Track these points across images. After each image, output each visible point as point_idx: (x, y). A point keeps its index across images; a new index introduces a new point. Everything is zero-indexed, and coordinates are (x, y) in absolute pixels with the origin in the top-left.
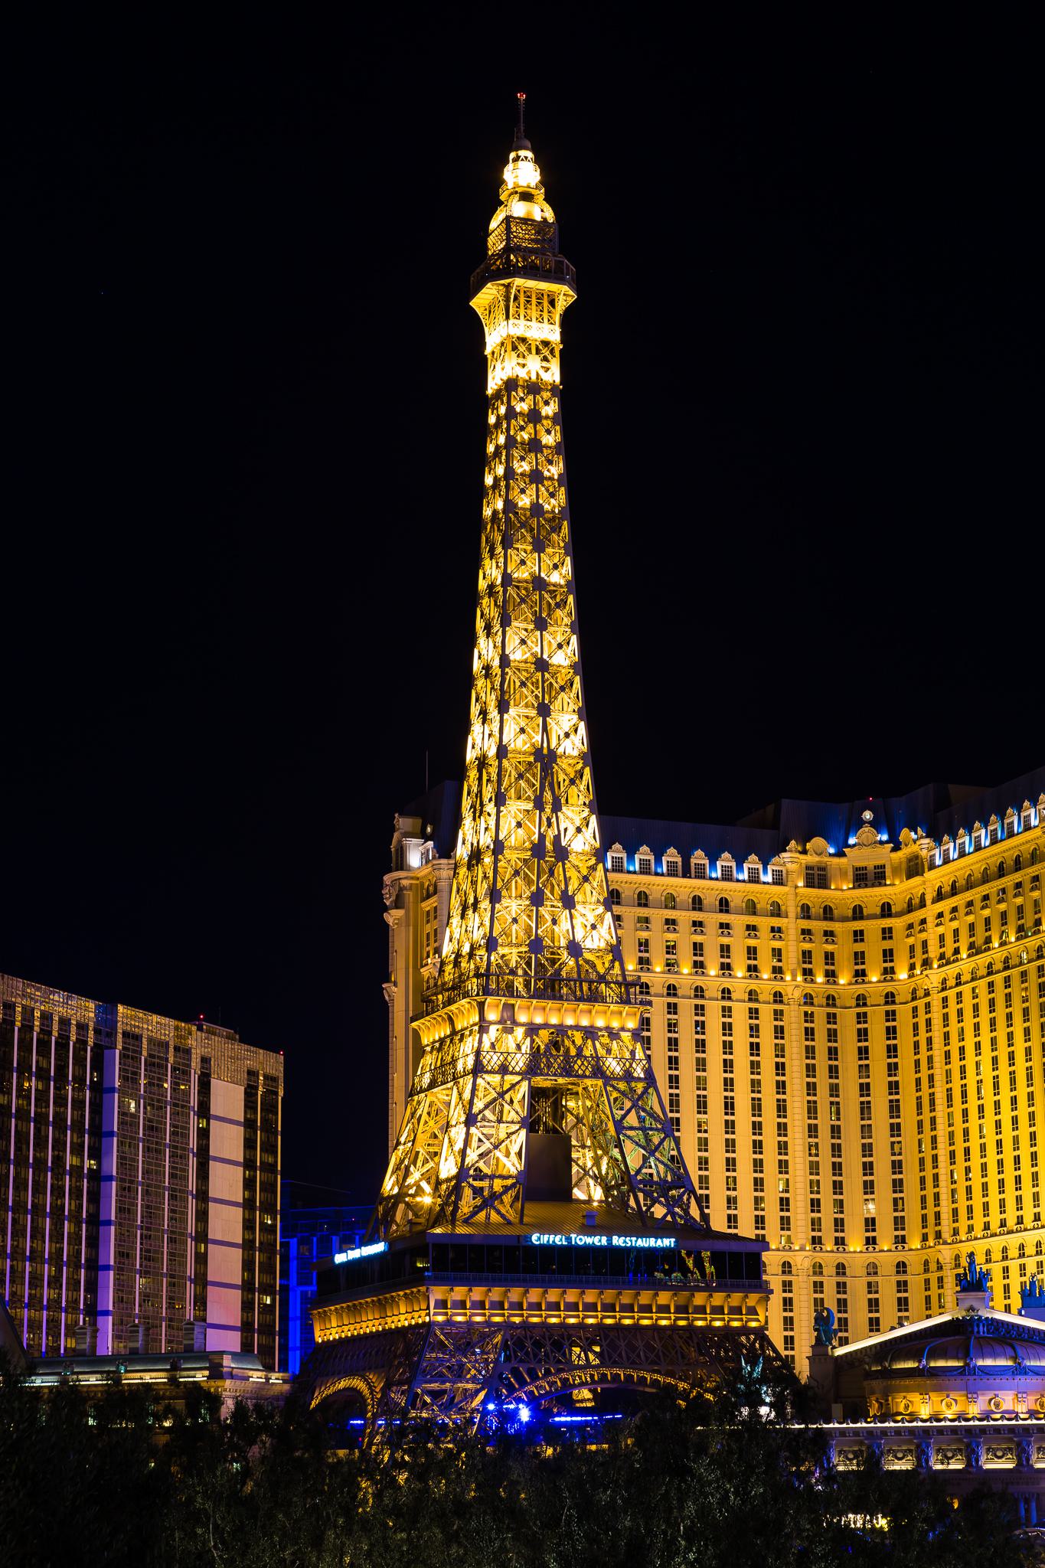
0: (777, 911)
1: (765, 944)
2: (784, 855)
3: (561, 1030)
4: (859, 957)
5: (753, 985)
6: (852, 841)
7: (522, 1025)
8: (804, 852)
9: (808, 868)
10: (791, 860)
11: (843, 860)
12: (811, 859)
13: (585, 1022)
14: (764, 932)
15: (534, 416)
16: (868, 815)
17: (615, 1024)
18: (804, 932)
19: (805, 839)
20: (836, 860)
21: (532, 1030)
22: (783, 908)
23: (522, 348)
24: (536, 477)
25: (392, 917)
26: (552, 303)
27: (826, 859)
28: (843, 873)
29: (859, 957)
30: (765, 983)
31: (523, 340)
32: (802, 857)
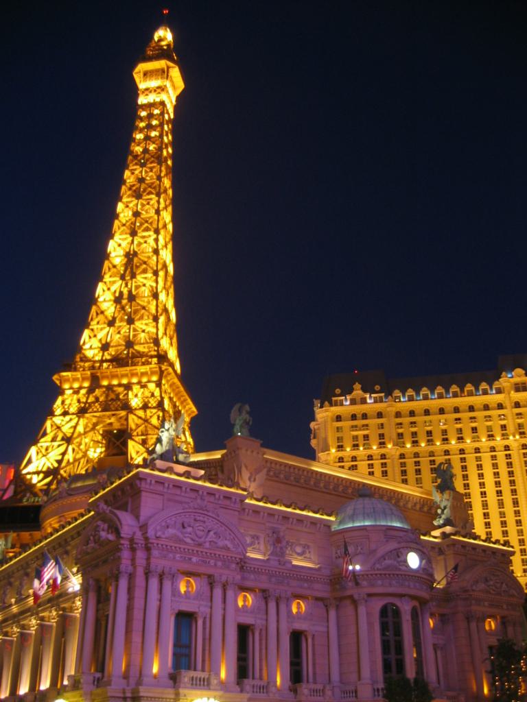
0: (500, 406)
1: (496, 424)
2: (500, 380)
5: (492, 443)
7: (85, 388)
8: (512, 377)
9: (516, 384)
12: (517, 380)
13: (125, 381)
14: (495, 418)
15: (150, 116)
17: (144, 380)
18: (517, 414)
22: (504, 405)
23: (146, 93)
24: (147, 138)
25: (313, 443)
26: (163, 72)
30: (499, 441)
31: (147, 89)
32: (511, 379)
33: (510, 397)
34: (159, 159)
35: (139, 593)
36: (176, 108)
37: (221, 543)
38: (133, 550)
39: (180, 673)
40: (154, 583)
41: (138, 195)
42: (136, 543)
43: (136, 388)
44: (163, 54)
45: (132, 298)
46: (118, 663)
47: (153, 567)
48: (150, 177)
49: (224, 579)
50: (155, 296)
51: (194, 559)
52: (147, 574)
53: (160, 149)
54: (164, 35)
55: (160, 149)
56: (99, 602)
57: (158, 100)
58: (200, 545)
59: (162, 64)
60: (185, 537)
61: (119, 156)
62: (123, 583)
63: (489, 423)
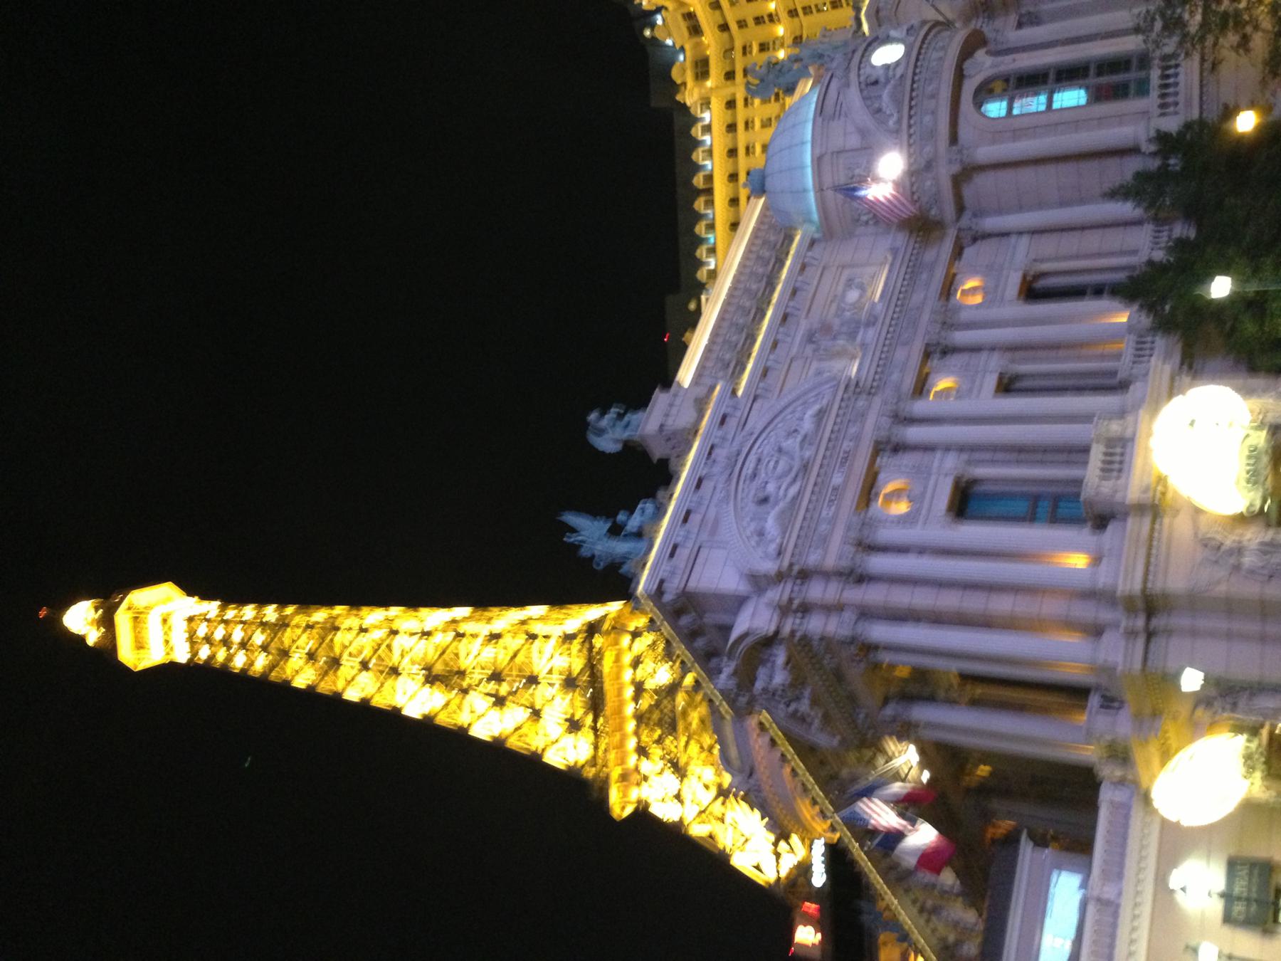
2: (688, 104)
3: (640, 718)
4: (759, 20)
6: (669, 42)
8: (684, 84)
10: (690, 97)
11: (687, 47)
13: (629, 691)
15: (208, 639)
16: (647, 33)
19: (674, 88)
20: (688, 53)
21: (642, 751)
27: (688, 64)
28: (699, 45)
29: (759, 20)
33: (717, 87)
34: (283, 624)
35: (902, 597)
36: (206, 596)
37: (807, 425)
38: (805, 609)
39: (1090, 504)
40: (879, 563)
41: (335, 663)
42: (791, 600)
43: (641, 673)
44: (107, 622)
45: (496, 677)
46: (1066, 654)
47: (845, 563)
48: (306, 642)
49: (886, 422)
50: (495, 637)
51: (837, 479)
52: (862, 578)
53: (264, 625)
54: (80, 619)
55: (264, 625)
56: (931, 699)
57: (184, 625)
58: (806, 467)
59: (122, 618)
60: (785, 496)
61: (268, 694)
62: (880, 632)
63: (758, 124)
